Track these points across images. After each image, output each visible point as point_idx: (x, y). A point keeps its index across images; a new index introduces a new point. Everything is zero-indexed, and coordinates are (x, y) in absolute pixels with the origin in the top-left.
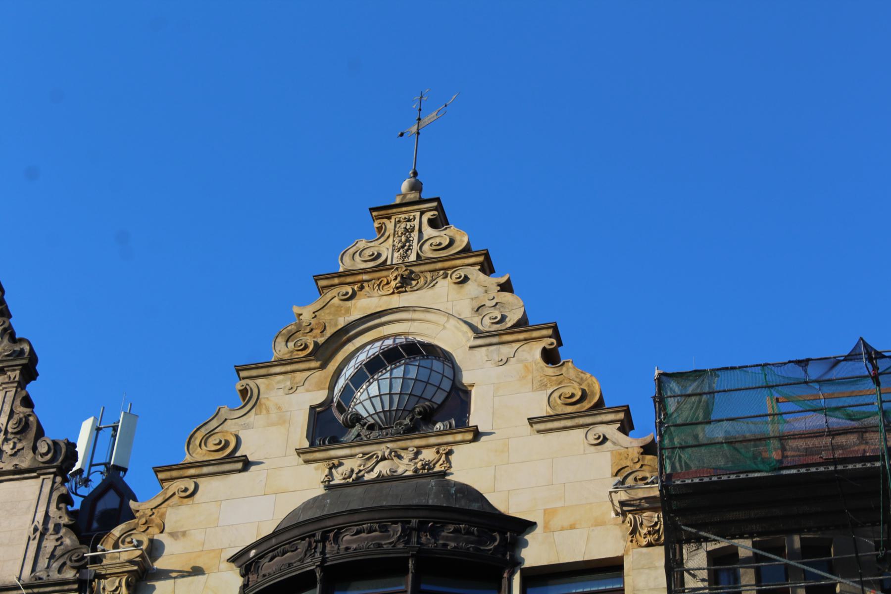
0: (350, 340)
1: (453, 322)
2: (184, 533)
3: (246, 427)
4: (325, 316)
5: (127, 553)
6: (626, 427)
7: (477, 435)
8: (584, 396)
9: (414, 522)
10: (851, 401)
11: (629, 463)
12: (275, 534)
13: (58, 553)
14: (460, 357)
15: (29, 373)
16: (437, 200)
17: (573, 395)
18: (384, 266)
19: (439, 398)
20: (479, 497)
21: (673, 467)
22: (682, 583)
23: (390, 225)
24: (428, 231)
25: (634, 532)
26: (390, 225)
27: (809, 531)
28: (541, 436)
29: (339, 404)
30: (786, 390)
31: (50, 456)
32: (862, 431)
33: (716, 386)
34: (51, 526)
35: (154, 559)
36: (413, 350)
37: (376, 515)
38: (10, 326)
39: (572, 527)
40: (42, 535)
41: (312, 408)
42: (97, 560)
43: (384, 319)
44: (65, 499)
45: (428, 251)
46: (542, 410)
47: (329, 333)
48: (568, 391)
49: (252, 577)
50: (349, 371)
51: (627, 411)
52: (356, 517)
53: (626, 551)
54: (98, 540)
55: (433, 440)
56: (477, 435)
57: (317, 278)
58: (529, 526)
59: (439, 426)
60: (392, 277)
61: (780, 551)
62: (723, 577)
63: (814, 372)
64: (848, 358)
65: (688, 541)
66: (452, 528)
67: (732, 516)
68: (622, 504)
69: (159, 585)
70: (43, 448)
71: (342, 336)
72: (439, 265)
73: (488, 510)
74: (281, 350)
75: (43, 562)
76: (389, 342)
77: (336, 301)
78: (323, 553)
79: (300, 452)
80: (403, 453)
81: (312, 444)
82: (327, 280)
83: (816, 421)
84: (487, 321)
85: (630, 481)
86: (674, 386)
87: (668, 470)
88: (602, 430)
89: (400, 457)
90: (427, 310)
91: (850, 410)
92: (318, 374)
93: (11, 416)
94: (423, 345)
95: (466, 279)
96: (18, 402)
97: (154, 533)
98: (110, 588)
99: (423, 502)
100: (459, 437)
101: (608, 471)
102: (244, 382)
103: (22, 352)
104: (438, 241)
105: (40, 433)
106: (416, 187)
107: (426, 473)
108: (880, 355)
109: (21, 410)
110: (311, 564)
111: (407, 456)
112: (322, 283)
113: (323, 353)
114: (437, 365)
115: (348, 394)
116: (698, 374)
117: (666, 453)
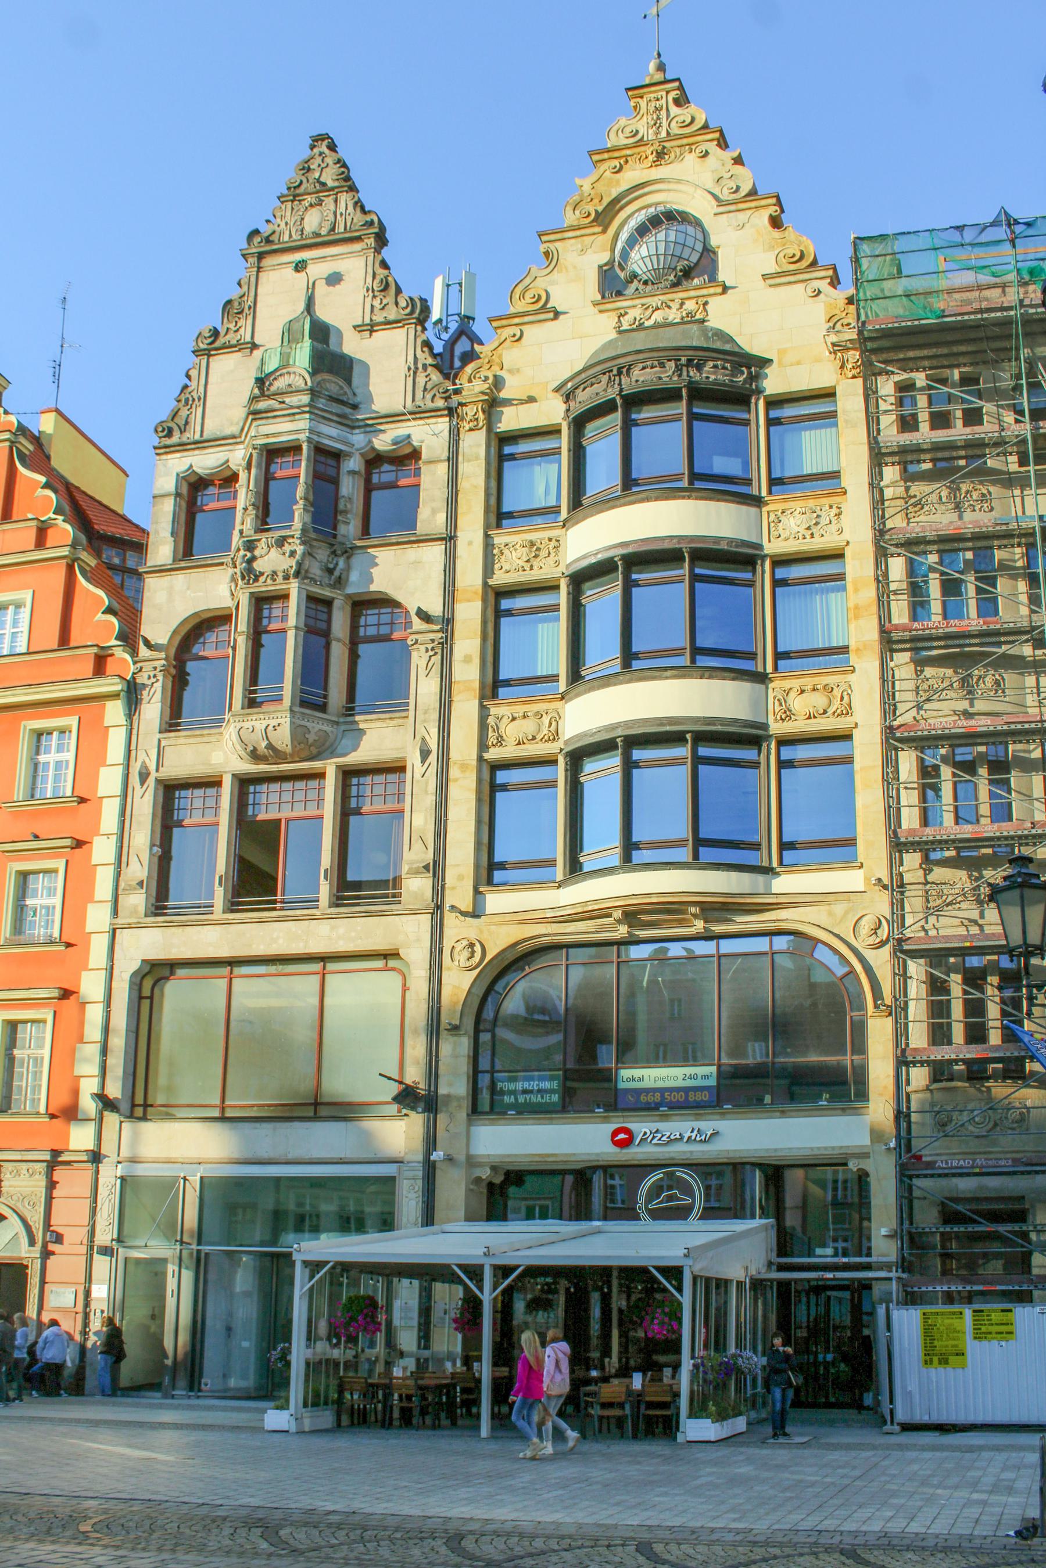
0: (622, 208)
1: (699, 192)
2: (518, 370)
3: (553, 283)
4: (601, 187)
5: (479, 386)
6: (835, 282)
7: (725, 289)
8: (802, 257)
9: (684, 360)
10: (993, 261)
11: (837, 312)
12: (584, 370)
13: (429, 386)
14: (707, 222)
15: (381, 240)
16: (678, 80)
17: (794, 256)
18: (641, 143)
19: (694, 258)
20: (731, 340)
21: (867, 316)
22: (877, 407)
23: (643, 103)
24: (674, 110)
25: (842, 367)
26: (643, 103)
27: (965, 365)
28: (772, 289)
29: (620, 264)
30: (948, 251)
31: (408, 310)
32: (1004, 286)
33: (896, 249)
34: (420, 366)
35: (499, 390)
36: (671, 216)
37: (655, 354)
38: (359, 200)
39: (798, 363)
40: (415, 373)
41: (600, 267)
42: (457, 392)
43: (646, 190)
44: (427, 344)
45: (675, 130)
46: (773, 268)
47: (606, 201)
48: (790, 252)
49: (572, 404)
50: (624, 236)
51: (835, 269)
52: (641, 356)
53: (838, 382)
54: (456, 376)
55: (692, 293)
56: (725, 289)
57: (591, 154)
58: (768, 362)
59: (696, 281)
60: (649, 152)
61: (944, 381)
62: (907, 402)
63: (969, 236)
64: (994, 224)
65: (880, 374)
66: (711, 364)
67: (911, 354)
68: (834, 345)
69: (505, 410)
70: (403, 303)
71: (614, 206)
72: (685, 141)
73: (737, 350)
74: (571, 218)
75: (419, 394)
76: (652, 210)
77: (608, 174)
78: (620, 384)
79: (595, 304)
80: (671, 304)
81: (603, 297)
82: (599, 154)
83: (968, 278)
84: (726, 191)
85: (838, 327)
86: (865, 248)
87: (863, 318)
88: (817, 284)
89: (669, 307)
90: (679, 181)
91: (993, 269)
92: (601, 237)
93: (374, 277)
94: (680, 213)
95: (707, 153)
96: (377, 265)
97: (496, 369)
98: (471, 414)
99: (689, 344)
100: (712, 291)
101: (823, 318)
102: (546, 245)
103: (372, 223)
104: (680, 119)
105: (399, 291)
106: (661, 68)
107: (690, 320)
108: (1016, 222)
109: (382, 273)
110: (612, 393)
111: (675, 306)
112: (595, 158)
113: (603, 218)
114: (690, 230)
115: (625, 255)
116: (883, 237)
117: (862, 304)
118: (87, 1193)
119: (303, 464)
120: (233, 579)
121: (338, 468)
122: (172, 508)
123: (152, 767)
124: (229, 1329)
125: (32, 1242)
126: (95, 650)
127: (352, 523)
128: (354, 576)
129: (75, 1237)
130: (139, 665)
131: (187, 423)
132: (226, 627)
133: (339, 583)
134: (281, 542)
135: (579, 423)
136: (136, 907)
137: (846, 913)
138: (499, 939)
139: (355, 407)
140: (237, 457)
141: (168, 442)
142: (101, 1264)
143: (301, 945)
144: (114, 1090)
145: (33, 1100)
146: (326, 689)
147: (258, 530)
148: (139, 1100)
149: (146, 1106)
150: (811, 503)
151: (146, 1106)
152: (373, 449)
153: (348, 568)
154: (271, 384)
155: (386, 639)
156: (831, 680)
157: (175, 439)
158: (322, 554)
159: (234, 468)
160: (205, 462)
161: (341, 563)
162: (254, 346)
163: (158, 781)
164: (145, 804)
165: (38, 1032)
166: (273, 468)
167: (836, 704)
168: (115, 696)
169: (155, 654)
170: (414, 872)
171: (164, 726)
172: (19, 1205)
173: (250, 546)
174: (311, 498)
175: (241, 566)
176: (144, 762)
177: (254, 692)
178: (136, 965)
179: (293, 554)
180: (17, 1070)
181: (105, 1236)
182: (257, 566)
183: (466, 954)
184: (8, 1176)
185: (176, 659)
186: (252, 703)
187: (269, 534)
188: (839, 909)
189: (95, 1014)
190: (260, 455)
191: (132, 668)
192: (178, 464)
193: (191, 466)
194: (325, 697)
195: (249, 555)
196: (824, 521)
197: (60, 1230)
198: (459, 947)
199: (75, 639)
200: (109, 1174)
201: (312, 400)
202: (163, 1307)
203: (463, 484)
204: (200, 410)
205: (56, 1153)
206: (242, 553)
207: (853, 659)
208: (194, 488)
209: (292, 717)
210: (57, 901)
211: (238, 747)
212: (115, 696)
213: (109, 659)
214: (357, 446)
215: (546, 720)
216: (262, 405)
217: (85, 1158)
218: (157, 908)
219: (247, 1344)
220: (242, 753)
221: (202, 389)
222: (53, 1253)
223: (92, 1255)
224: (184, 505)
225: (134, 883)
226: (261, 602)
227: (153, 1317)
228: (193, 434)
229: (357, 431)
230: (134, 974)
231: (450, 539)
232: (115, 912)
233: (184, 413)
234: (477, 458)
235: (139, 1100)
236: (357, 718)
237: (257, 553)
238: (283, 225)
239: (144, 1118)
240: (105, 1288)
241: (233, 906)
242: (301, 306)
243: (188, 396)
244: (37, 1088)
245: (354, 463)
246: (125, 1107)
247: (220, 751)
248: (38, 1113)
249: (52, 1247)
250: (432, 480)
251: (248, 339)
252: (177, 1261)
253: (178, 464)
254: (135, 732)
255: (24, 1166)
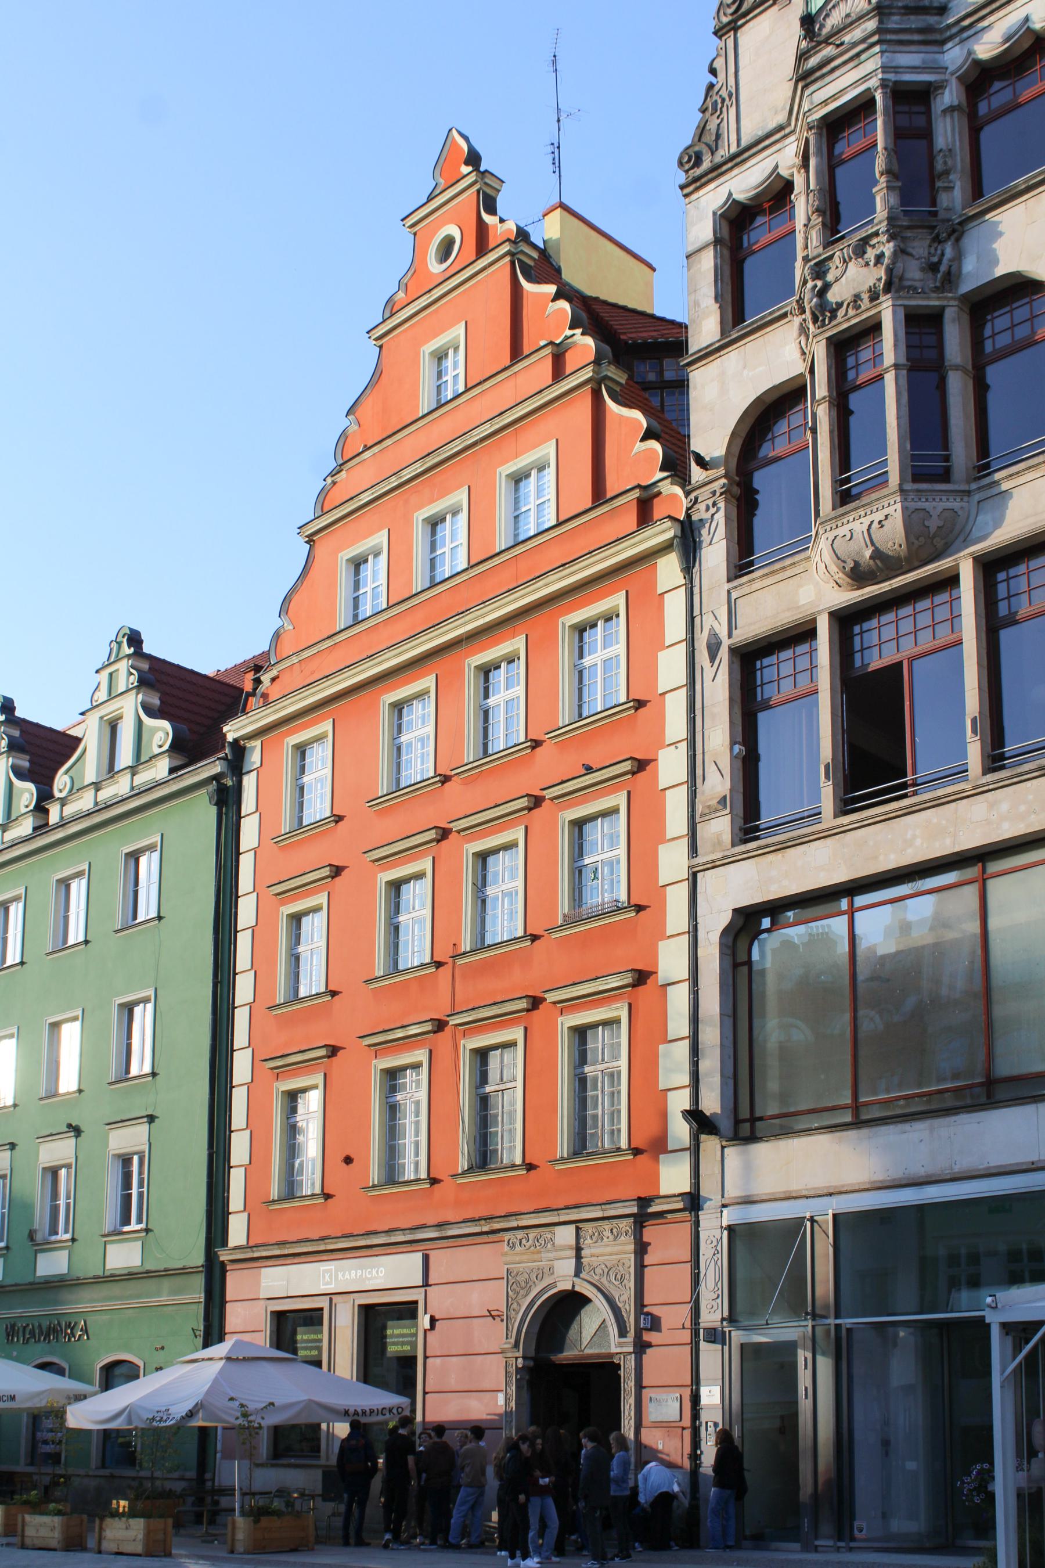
118: (687, 1255)
119: (880, 122)
120: (803, 330)
121: (928, 113)
122: (712, 264)
123: (723, 632)
124: (886, 1443)
125: (623, 1332)
126: (636, 494)
127: (958, 184)
128: (969, 265)
129: (674, 1319)
130: (692, 496)
131: (718, 136)
132: (801, 407)
133: (950, 279)
134: (860, 250)
136: (719, 835)
141: (698, 172)
142: (711, 1355)
143: (948, 841)
144: (711, 1103)
145: (612, 1132)
146: (946, 447)
147: (827, 244)
148: (745, 1113)
149: (753, 1120)
151: (753, 1120)
152: (977, 63)
153: (959, 257)
154: (822, 26)
155: (1029, 343)
157: (706, 165)
158: (920, 247)
159: (784, 172)
161: (949, 250)
163: (733, 651)
164: (718, 687)
165: (612, 1037)
166: (839, 148)
168: (664, 549)
169: (712, 473)
171: (733, 571)
172: (604, 1280)
173: (819, 270)
174: (895, 167)
175: (810, 302)
176: (712, 629)
177: (848, 480)
178: (725, 919)
179: (879, 258)
180: (590, 1093)
181: (712, 1315)
182: (833, 296)
184: (589, 1241)
185: (739, 472)
186: (844, 497)
187: (840, 245)
189: (678, 999)
190: (819, 135)
191: (685, 503)
192: (713, 198)
193: (730, 194)
194: (947, 458)
195: (819, 283)
197: (655, 1311)
199: (613, 485)
200: (713, 1226)
201: (880, 22)
202: (795, 1415)
204: (733, 111)
205: (644, 1202)
206: (810, 284)
208: (737, 222)
209: (904, 500)
210: (622, 852)
211: (833, 569)
212: (664, 549)
213: (656, 501)
214: (951, 68)
216: (813, 62)
217: (680, 1205)
218: (747, 831)
219: (913, 1465)
220: (840, 576)
222: (649, 1345)
223: (697, 1344)
224: (727, 253)
225: (714, 802)
226: (842, 348)
227: (782, 1431)
228: (729, 146)
229: (950, 45)
230: (725, 932)
232: (694, 850)
235: (745, 1113)
236: (997, 476)
237: (830, 277)
239: (752, 1138)
240: (716, 1390)
241: (846, 806)
243: (717, 101)
244: (615, 1115)
245: (950, 96)
246: (726, 1125)
247: (810, 587)
248: (619, 1149)
249: (647, 1337)
252: (809, 1344)
253: (713, 198)
254: (696, 590)
255: (607, 1225)
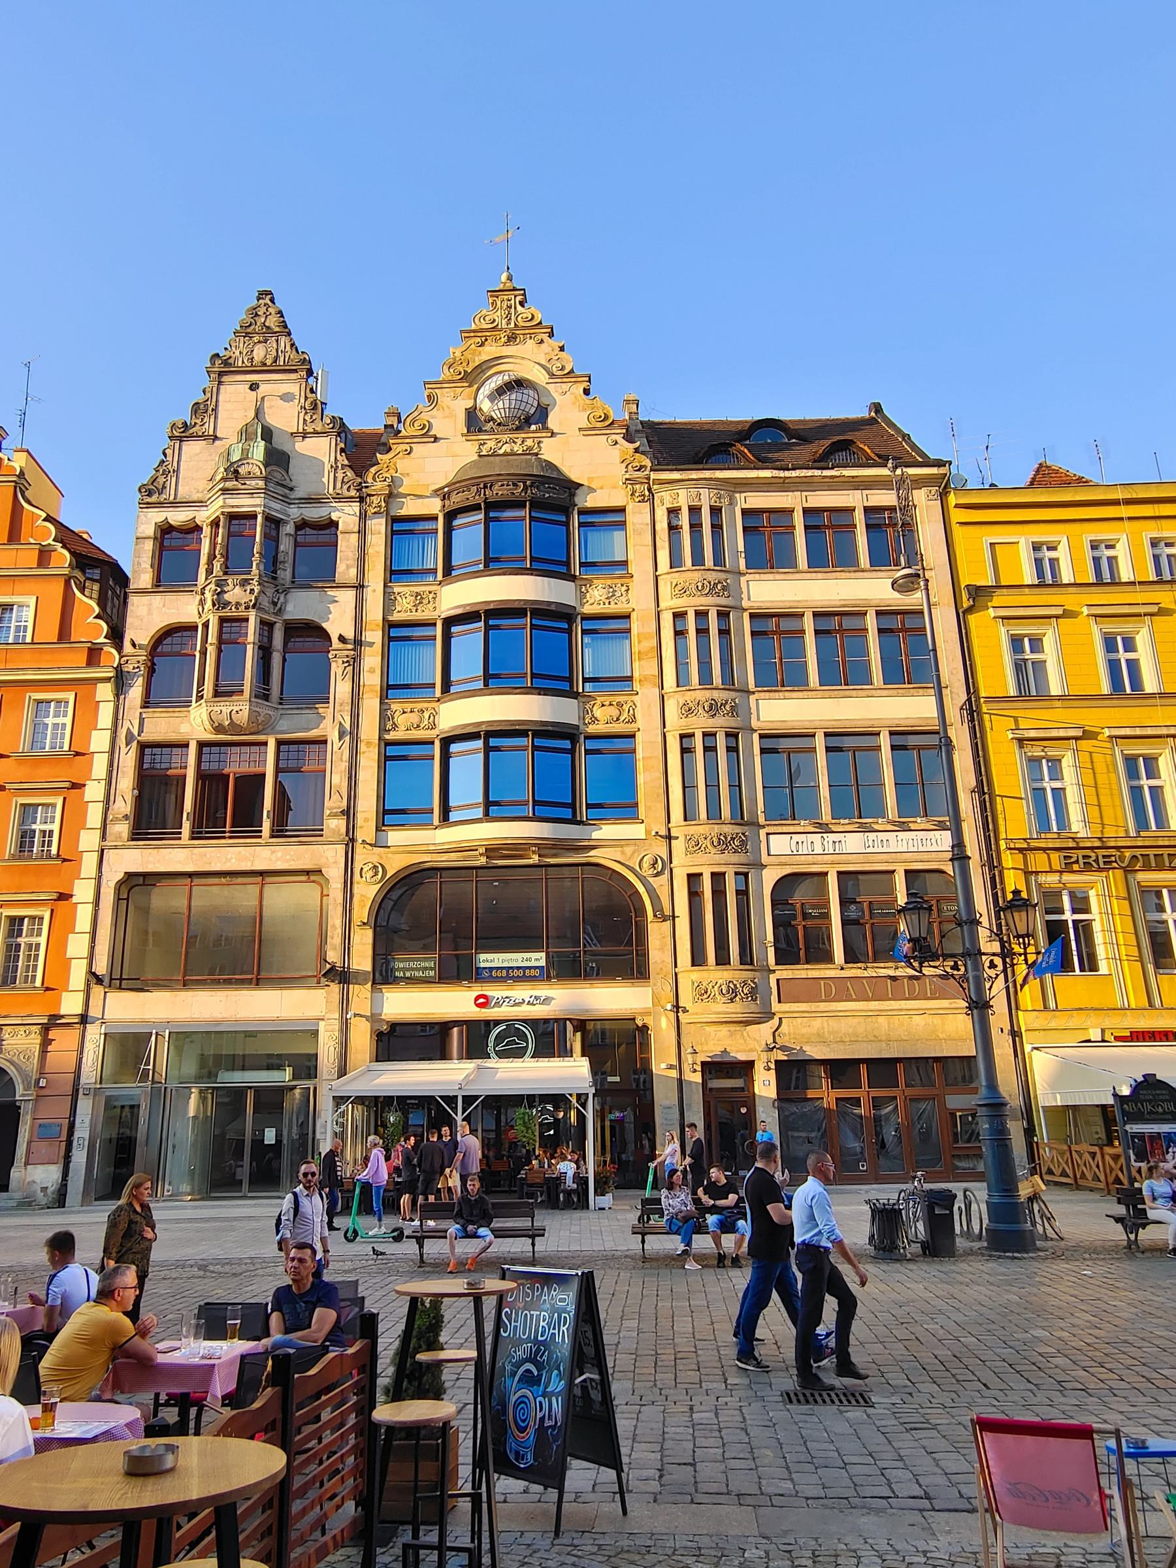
24: (519, 308)
46: (585, 424)
49: (447, 502)
56: (553, 434)
59: (533, 427)
74: (446, 374)
75: (339, 485)
84: (554, 369)
101: (618, 460)
104: (524, 315)
106: (510, 278)
107: (528, 452)
123: (136, 733)
128: (290, 607)
135: (450, 516)
137: (634, 853)
138: (395, 864)
139: (291, 489)
140: (203, 516)
141: (149, 500)
150: (609, 582)
153: (286, 602)
156: (621, 699)
157: (154, 499)
160: (178, 517)
162: (216, 438)
167: (625, 716)
168: (108, 680)
170: (333, 815)
183: (371, 873)
188: (629, 850)
192: (157, 516)
196: (618, 594)
198: (366, 868)
203: (370, 551)
204: (174, 479)
207: (637, 686)
212: (108, 680)
215: (426, 715)
221: (175, 464)
231: (360, 587)
233: (161, 480)
234: (379, 533)
238: (237, 353)
242: (252, 414)
243: (166, 469)
245: (289, 528)
250: (347, 546)
251: (211, 433)
253: (157, 516)
